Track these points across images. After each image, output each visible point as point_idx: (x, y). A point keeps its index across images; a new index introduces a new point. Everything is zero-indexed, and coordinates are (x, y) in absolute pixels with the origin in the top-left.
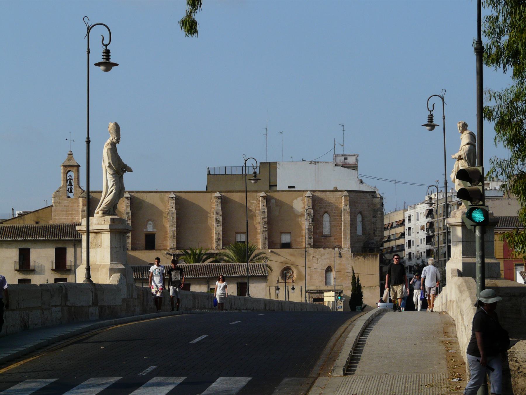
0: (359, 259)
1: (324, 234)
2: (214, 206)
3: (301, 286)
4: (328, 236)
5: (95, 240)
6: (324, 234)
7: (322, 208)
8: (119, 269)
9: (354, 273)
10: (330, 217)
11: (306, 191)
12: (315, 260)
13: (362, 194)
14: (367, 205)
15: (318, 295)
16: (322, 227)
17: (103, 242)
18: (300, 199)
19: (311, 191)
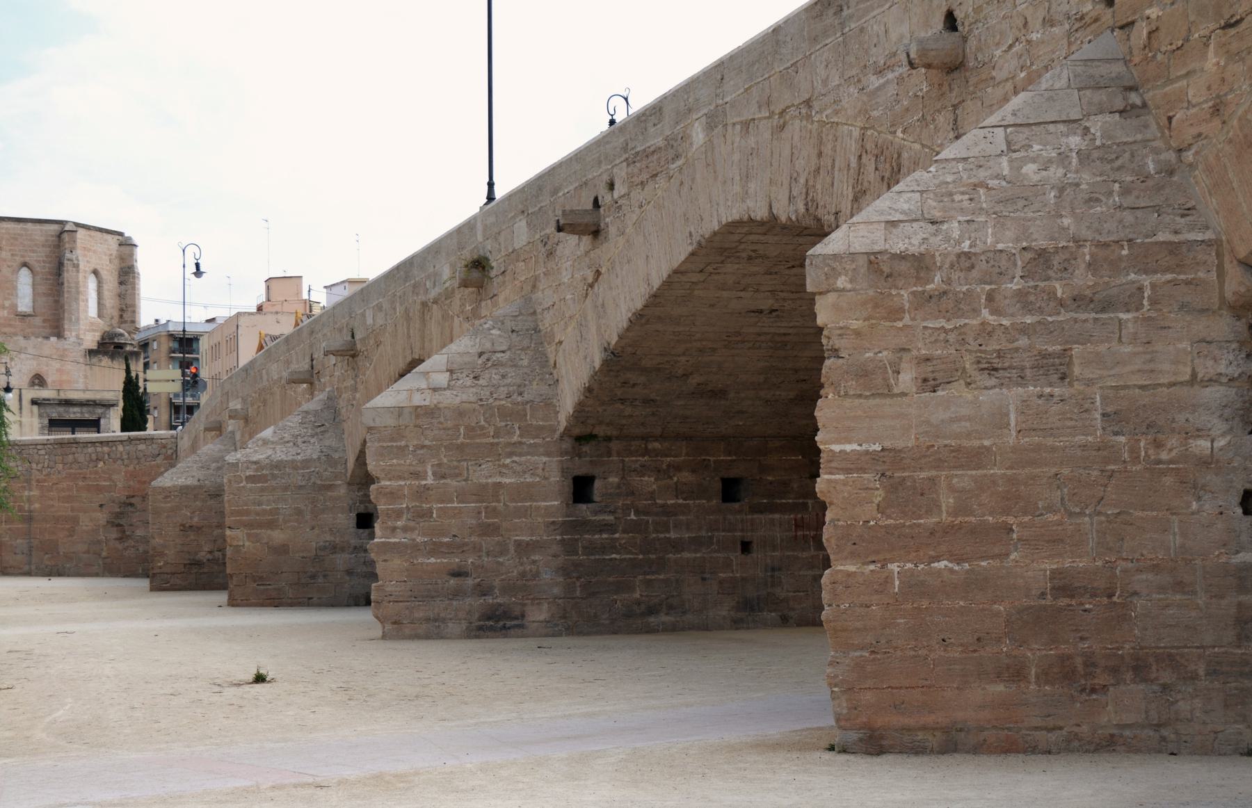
0: (100, 361)
1: (19, 309)
3: (20, 389)
4: (29, 315)
6: (19, 309)
7: (16, 255)
10: (33, 278)
13: (99, 233)
14: (107, 258)
15: (61, 409)
16: (17, 296)
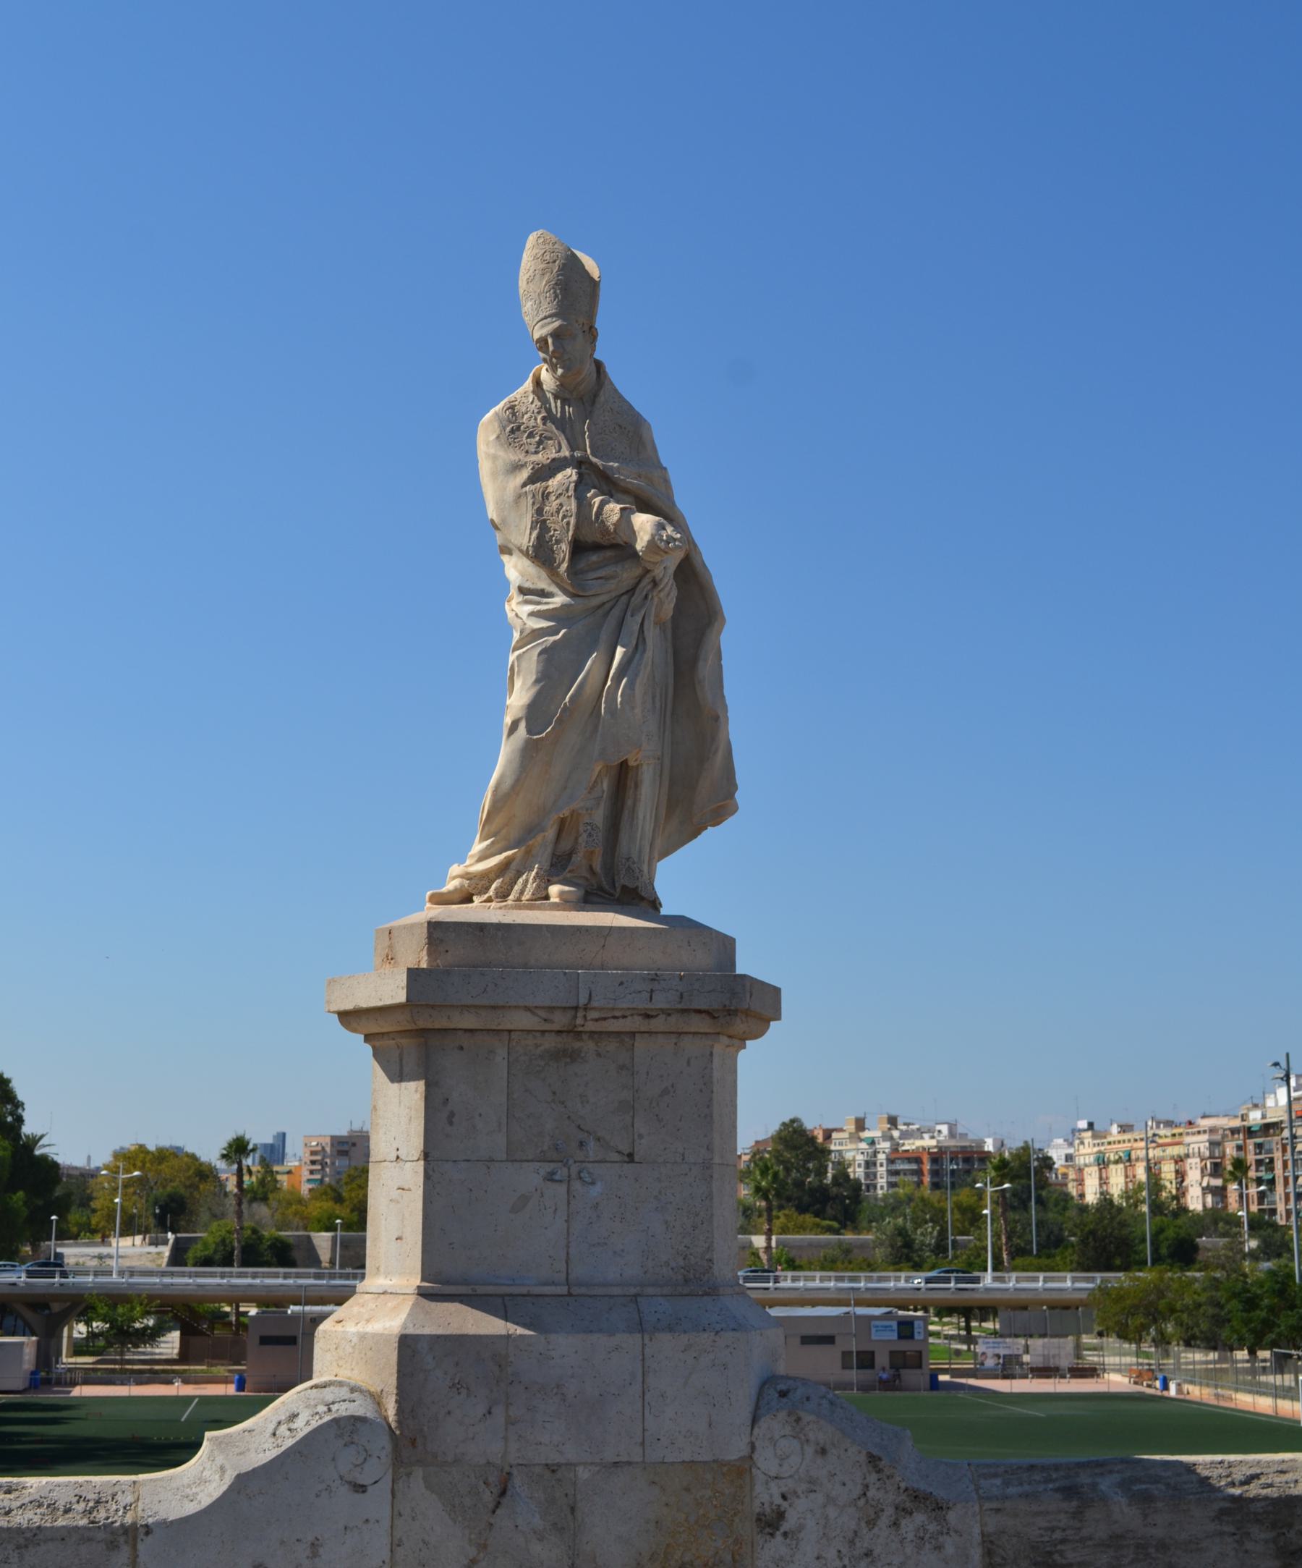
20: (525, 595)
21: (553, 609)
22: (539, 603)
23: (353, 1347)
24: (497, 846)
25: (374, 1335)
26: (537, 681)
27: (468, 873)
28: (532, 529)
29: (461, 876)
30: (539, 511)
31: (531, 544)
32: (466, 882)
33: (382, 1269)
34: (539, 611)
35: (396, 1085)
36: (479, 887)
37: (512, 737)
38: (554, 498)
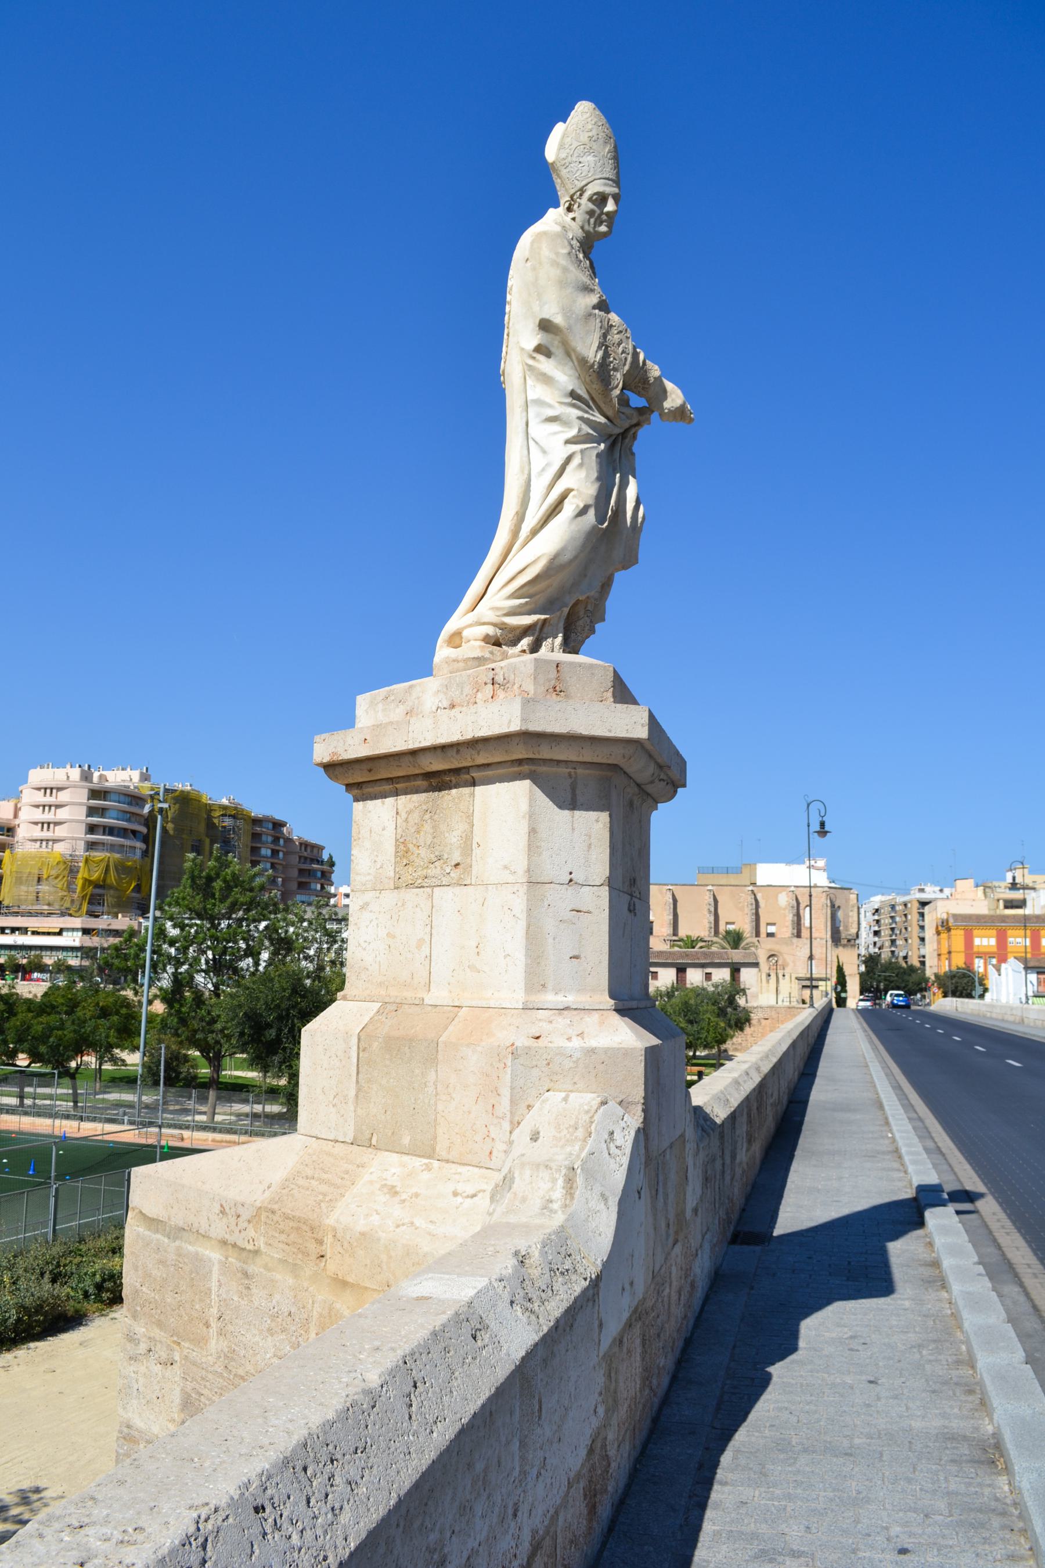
2: (707, 898)
5: (427, 827)
8: (593, 1051)
9: (838, 962)
11: (788, 886)
12: (798, 949)
17: (476, 839)
18: (784, 893)
19: (795, 886)
20: (574, 399)
21: (596, 421)
22: (587, 412)
23: (576, 1062)
24: (528, 607)
25: (606, 1050)
26: (598, 479)
27: (504, 624)
28: (599, 348)
29: (495, 625)
30: (605, 336)
31: (597, 360)
32: (499, 632)
33: (550, 986)
34: (588, 419)
35: (566, 812)
36: (507, 638)
37: (579, 518)
38: (616, 332)
